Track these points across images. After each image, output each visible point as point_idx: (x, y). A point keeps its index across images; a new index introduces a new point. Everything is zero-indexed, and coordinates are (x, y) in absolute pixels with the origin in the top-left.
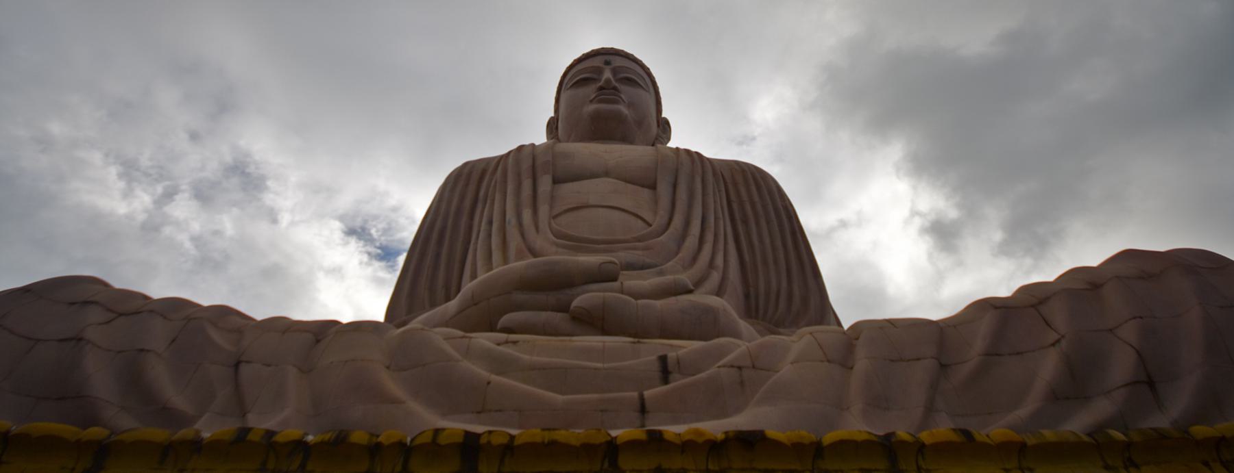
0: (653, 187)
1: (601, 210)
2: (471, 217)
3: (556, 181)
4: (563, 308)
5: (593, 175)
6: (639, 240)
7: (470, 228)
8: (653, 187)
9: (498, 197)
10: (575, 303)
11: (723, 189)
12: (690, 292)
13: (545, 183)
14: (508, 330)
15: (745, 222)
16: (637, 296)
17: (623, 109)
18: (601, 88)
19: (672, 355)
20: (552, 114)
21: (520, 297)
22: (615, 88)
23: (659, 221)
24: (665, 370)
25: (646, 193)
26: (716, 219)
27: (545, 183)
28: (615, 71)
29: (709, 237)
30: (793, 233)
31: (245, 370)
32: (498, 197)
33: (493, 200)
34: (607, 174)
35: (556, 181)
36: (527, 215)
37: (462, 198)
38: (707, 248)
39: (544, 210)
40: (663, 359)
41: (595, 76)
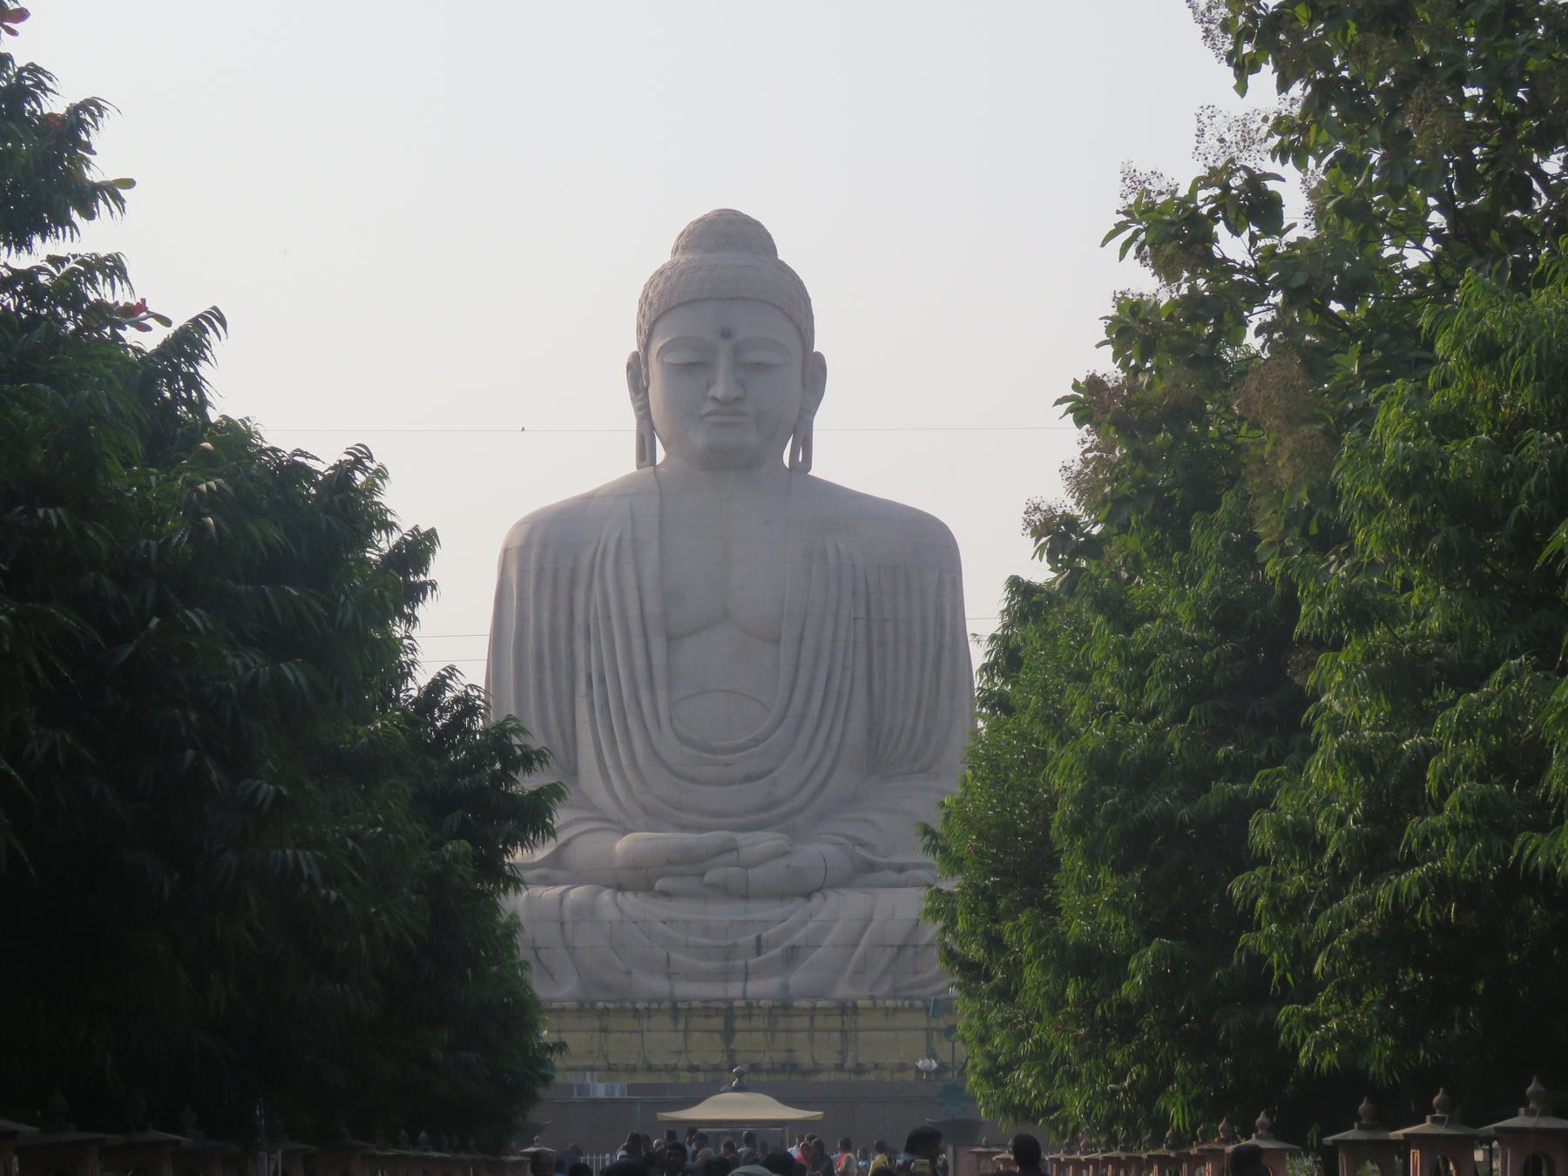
0: (777, 641)
2: (571, 640)
6: (756, 742)
10: (708, 878)
11: (862, 613)
12: (786, 854)
13: (658, 646)
16: (746, 866)
18: (715, 399)
19: (765, 935)
20: (632, 345)
22: (738, 399)
26: (844, 669)
30: (940, 647)
31: (542, 954)
33: (599, 641)
35: (670, 638)
36: (644, 695)
39: (661, 695)
40: (759, 938)
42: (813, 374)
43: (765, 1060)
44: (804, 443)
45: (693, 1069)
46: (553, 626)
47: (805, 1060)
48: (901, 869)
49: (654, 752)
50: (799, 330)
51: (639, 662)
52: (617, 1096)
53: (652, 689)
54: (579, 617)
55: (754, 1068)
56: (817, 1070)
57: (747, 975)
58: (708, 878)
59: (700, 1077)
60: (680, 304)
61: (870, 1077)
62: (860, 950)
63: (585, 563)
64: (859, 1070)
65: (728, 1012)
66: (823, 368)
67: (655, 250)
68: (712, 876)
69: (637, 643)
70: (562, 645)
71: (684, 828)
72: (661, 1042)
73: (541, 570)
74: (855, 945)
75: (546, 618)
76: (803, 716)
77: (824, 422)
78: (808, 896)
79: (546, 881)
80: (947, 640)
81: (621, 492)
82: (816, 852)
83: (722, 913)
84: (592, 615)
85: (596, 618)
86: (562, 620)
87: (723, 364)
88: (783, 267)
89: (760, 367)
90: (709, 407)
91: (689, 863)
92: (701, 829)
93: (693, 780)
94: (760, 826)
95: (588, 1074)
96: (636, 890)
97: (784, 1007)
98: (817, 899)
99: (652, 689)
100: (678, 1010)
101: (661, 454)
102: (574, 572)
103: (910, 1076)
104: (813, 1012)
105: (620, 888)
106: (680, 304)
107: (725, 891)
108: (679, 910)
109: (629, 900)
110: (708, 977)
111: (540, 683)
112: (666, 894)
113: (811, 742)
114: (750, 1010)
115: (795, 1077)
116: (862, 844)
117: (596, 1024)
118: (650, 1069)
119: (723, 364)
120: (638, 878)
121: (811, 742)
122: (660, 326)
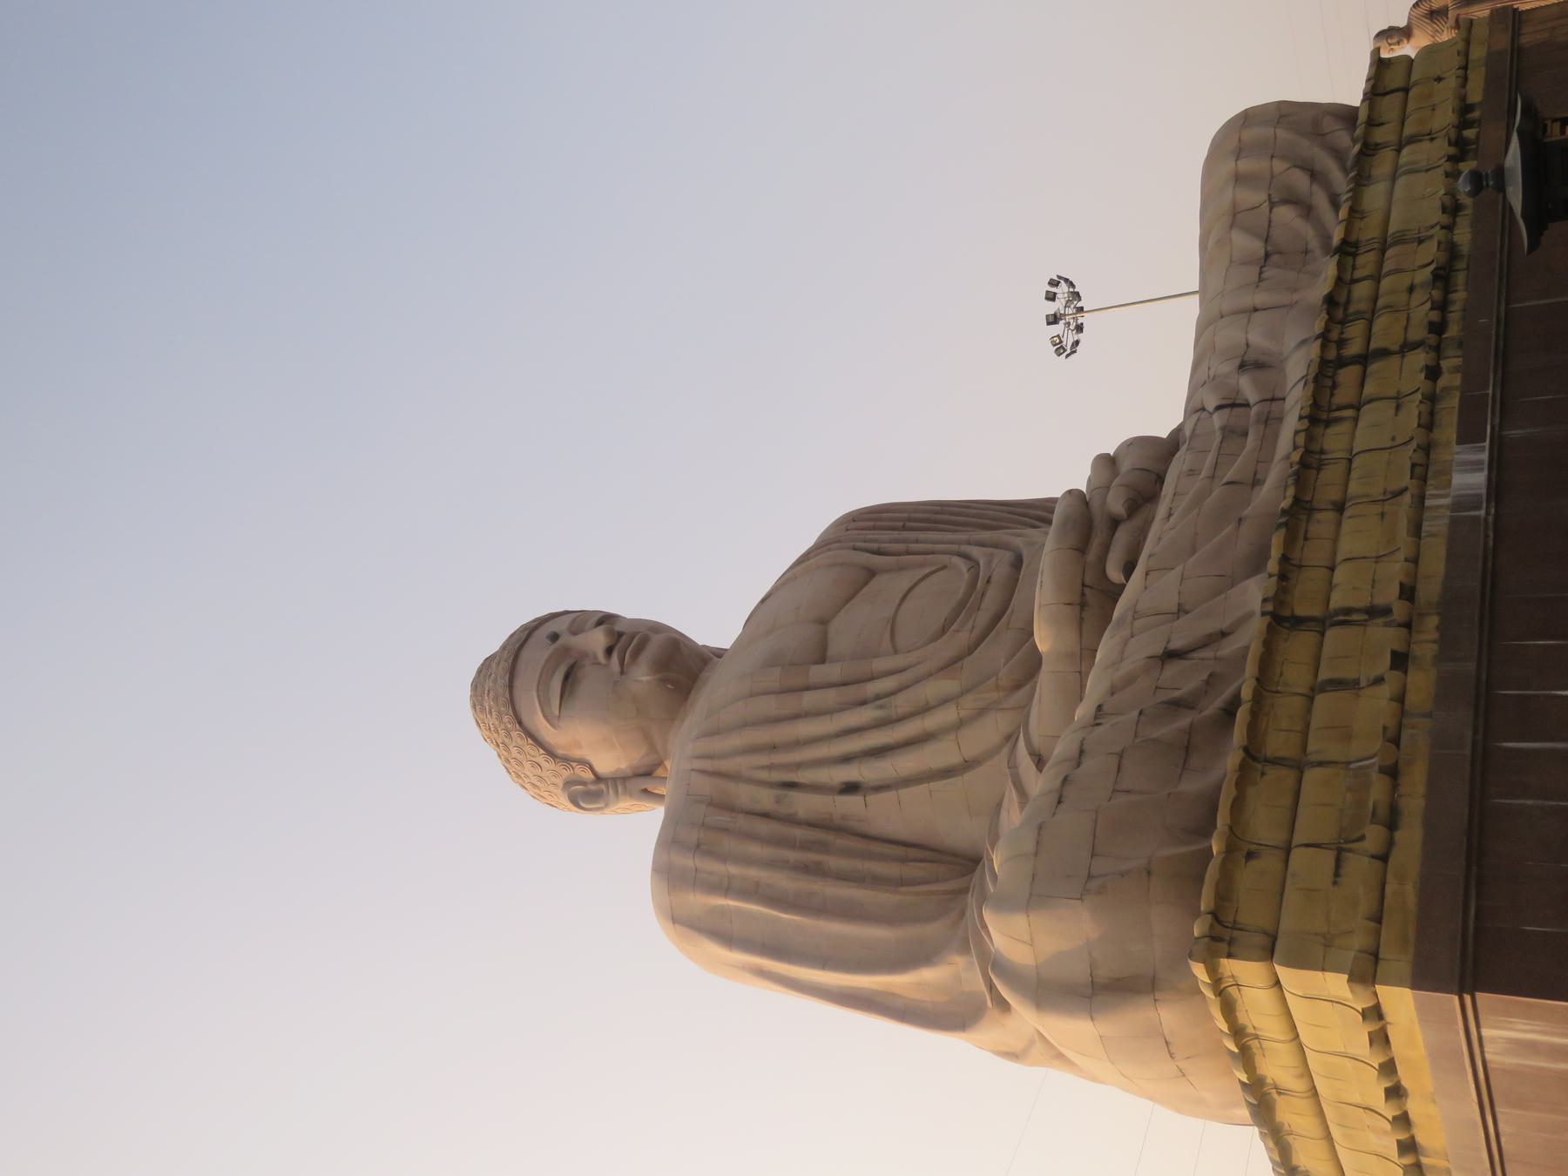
1: (906, 604)
4: (1115, 523)
7: (811, 824)
8: (871, 573)
14: (1129, 569)
18: (609, 651)
21: (1092, 556)
31: (1176, 644)
33: (800, 766)
34: (823, 622)
36: (873, 688)
39: (880, 664)
41: (570, 661)
43: (1422, 312)
49: (950, 665)
52: (1485, 456)
60: (511, 686)
63: (699, 764)
70: (798, 833)
75: (755, 849)
84: (763, 775)
85: (770, 767)
86: (764, 827)
95: (1428, 503)
106: (511, 686)
117: (1325, 518)
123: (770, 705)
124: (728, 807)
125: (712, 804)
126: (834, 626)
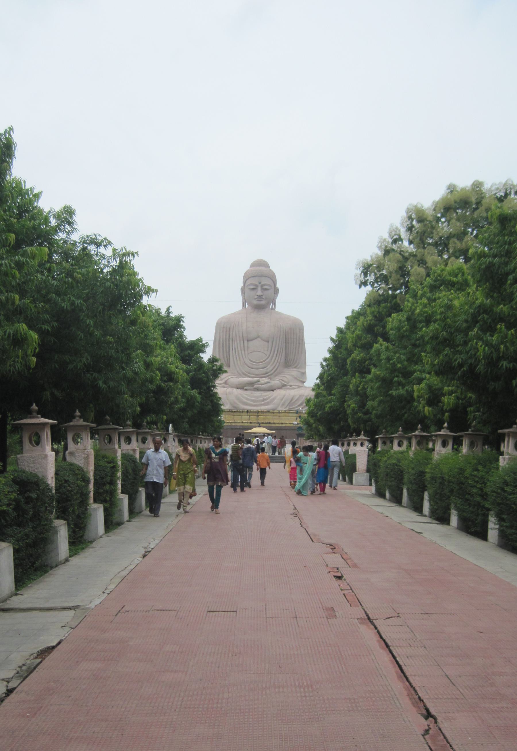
0: (268, 342)
3: (248, 341)
5: (256, 338)
7: (229, 344)
8: (268, 342)
9: (236, 343)
10: (254, 387)
13: (246, 342)
15: (288, 343)
17: (263, 302)
20: (242, 285)
23: (268, 354)
24: (264, 400)
25: (266, 343)
27: (246, 342)
28: (262, 286)
29: (278, 355)
30: (299, 343)
32: (236, 343)
34: (259, 337)
35: (248, 341)
37: (226, 335)
38: (277, 358)
39: (246, 352)
42: (276, 291)
44: (275, 304)
45: (251, 423)
46: (226, 339)
47: (272, 422)
48: (291, 386)
50: (274, 282)
51: (242, 345)
53: (244, 351)
54: (231, 337)
55: (263, 423)
56: (274, 423)
57: (261, 405)
58: (254, 387)
59: (252, 425)
61: (284, 425)
62: (283, 401)
64: (282, 424)
65: (258, 412)
66: (278, 290)
67: (246, 267)
68: (255, 386)
69: (242, 342)
70: (228, 342)
71: (250, 377)
72: (245, 418)
73: (224, 327)
74: (282, 400)
75: (224, 336)
76: (273, 356)
77: (278, 300)
78: (273, 391)
79: (224, 387)
80: (301, 342)
81: (239, 313)
82: (275, 382)
83: (258, 393)
87: (259, 288)
88: (271, 270)
89: (266, 289)
90: (257, 297)
91: (251, 384)
92: (253, 377)
93: (252, 368)
94: (264, 377)
96: (241, 389)
97: (269, 412)
98: (275, 391)
99: (244, 351)
100: (247, 412)
101: (247, 306)
102: (230, 328)
103: (292, 425)
104: (273, 413)
105: (238, 389)
107: (257, 389)
108: (248, 392)
109: (239, 391)
110: (254, 406)
111: (223, 349)
112: (246, 390)
113: (274, 361)
114: (262, 412)
115: (270, 425)
116: (283, 380)
118: (243, 423)
119: (259, 288)
120: (241, 387)
121: (274, 361)
122: (247, 281)
123: (241, 336)
124: (229, 331)
125: (230, 328)
126: (259, 339)
